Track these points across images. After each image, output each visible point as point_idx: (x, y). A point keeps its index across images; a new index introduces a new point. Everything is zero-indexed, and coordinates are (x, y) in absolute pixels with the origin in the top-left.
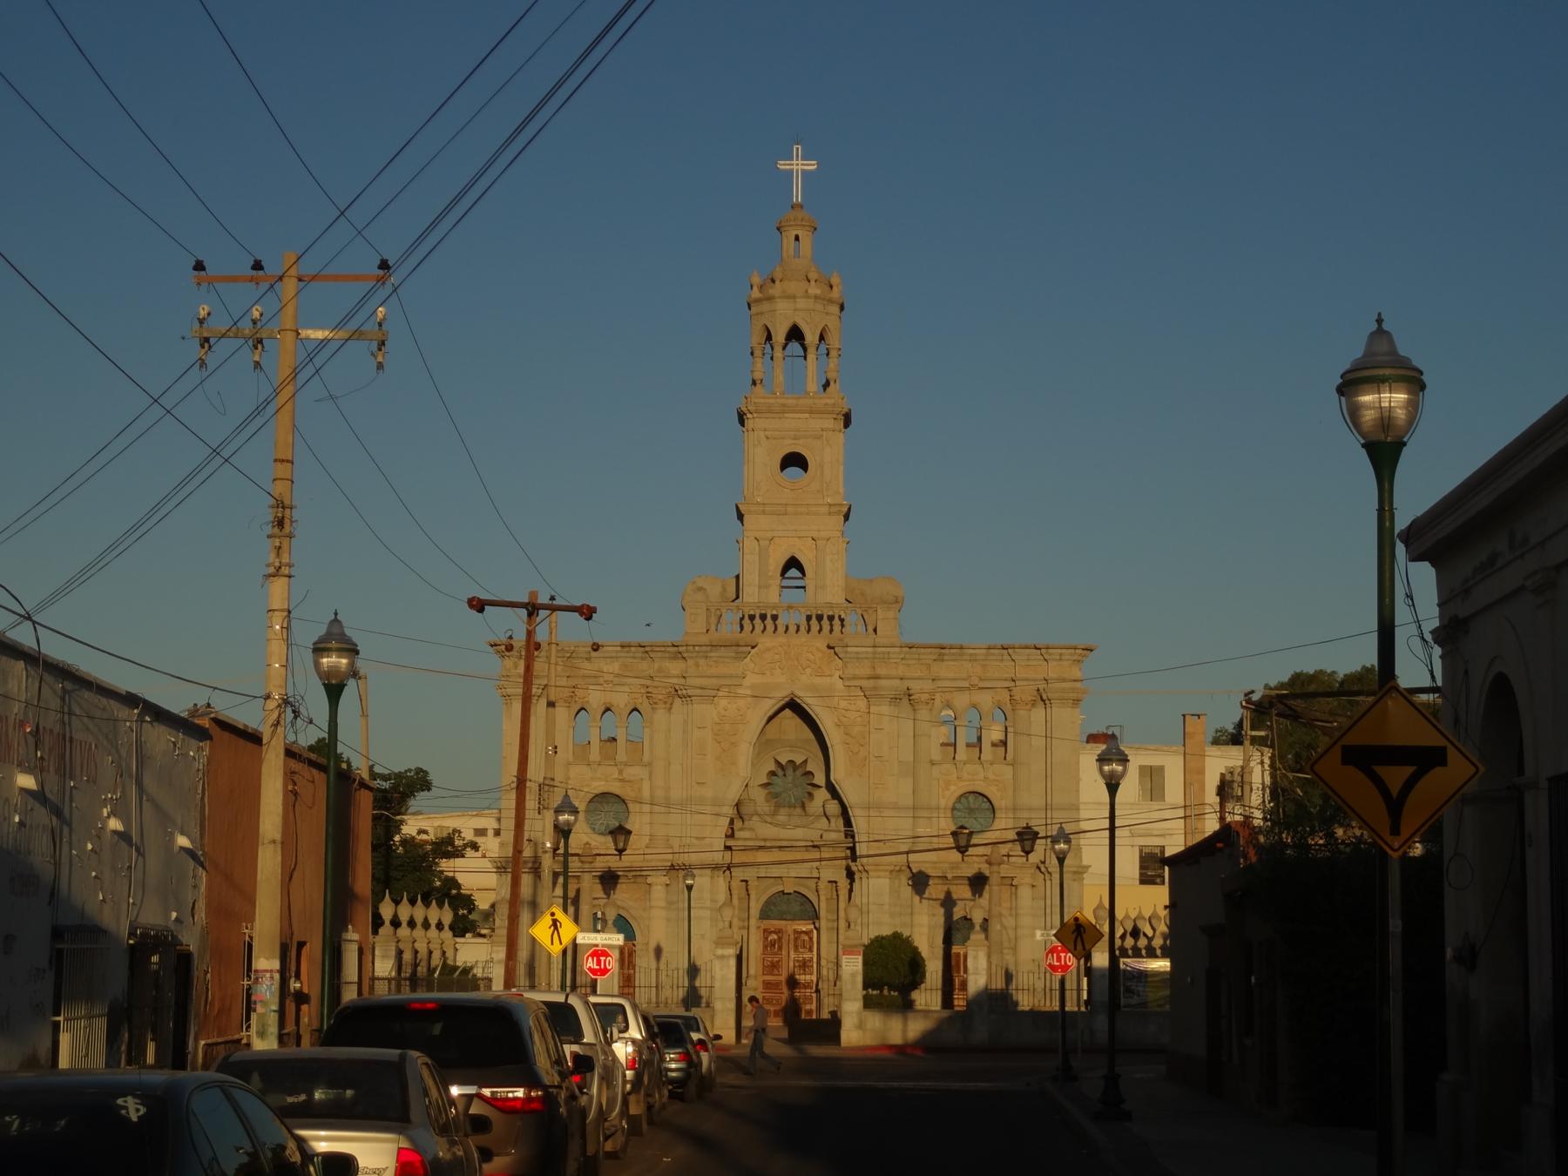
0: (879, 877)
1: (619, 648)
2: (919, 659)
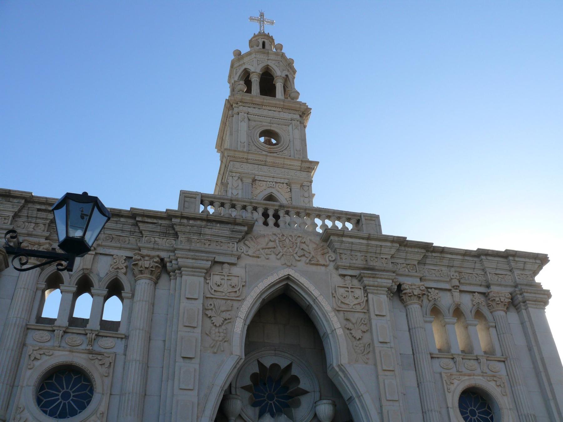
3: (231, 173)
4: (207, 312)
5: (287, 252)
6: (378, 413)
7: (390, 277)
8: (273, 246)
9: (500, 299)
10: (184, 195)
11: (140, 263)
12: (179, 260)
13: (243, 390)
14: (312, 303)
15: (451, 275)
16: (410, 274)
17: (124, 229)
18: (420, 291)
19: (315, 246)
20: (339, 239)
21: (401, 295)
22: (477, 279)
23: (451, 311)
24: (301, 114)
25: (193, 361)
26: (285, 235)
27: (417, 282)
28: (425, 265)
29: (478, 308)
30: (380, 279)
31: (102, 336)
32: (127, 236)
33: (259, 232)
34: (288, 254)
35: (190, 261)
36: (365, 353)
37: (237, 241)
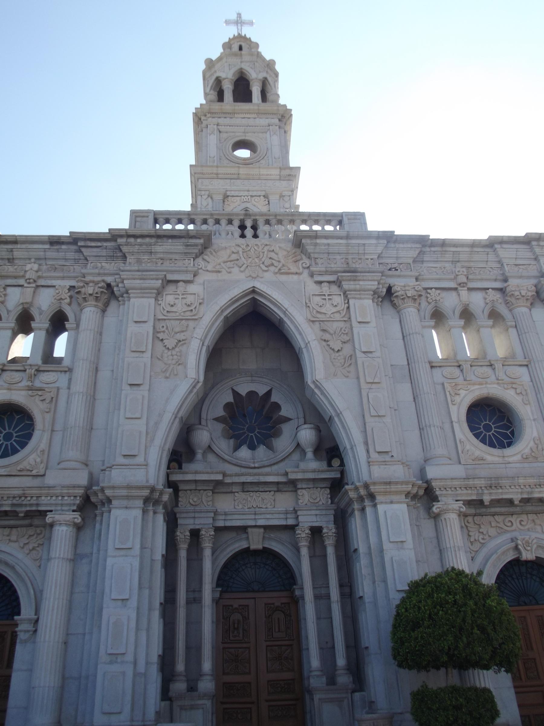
0: (392, 502)
1: (47, 246)
2: (397, 258)
3: (199, 192)
4: (159, 335)
5: (252, 263)
6: (361, 431)
7: (375, 278)
8: (236, 258)
9: (520, 293)
10: (135, 214)
11: (83, 290)
12: (125, 282)
13: (215, 422)
14: (282, 316)
15: (456, 272)
16: (402, 273)
17: (67, 257)
18: (415, 292)
19: (285, 253)
20: (312, 241)
21: (392, 299)
22: (491, 273)
23: (457, 313)
24: (280, 117)
25: (141, 388)
26: (250, 245)
27: (412, 282)
28: (423, 263)
29: (493, 306)
30: (363, 282)
31: (44, 371)
32: (72, 264)
33: (220, 245)
34: (254, 265)
35: (138, 281)
36: (346, 365)
37: (194, 256)
